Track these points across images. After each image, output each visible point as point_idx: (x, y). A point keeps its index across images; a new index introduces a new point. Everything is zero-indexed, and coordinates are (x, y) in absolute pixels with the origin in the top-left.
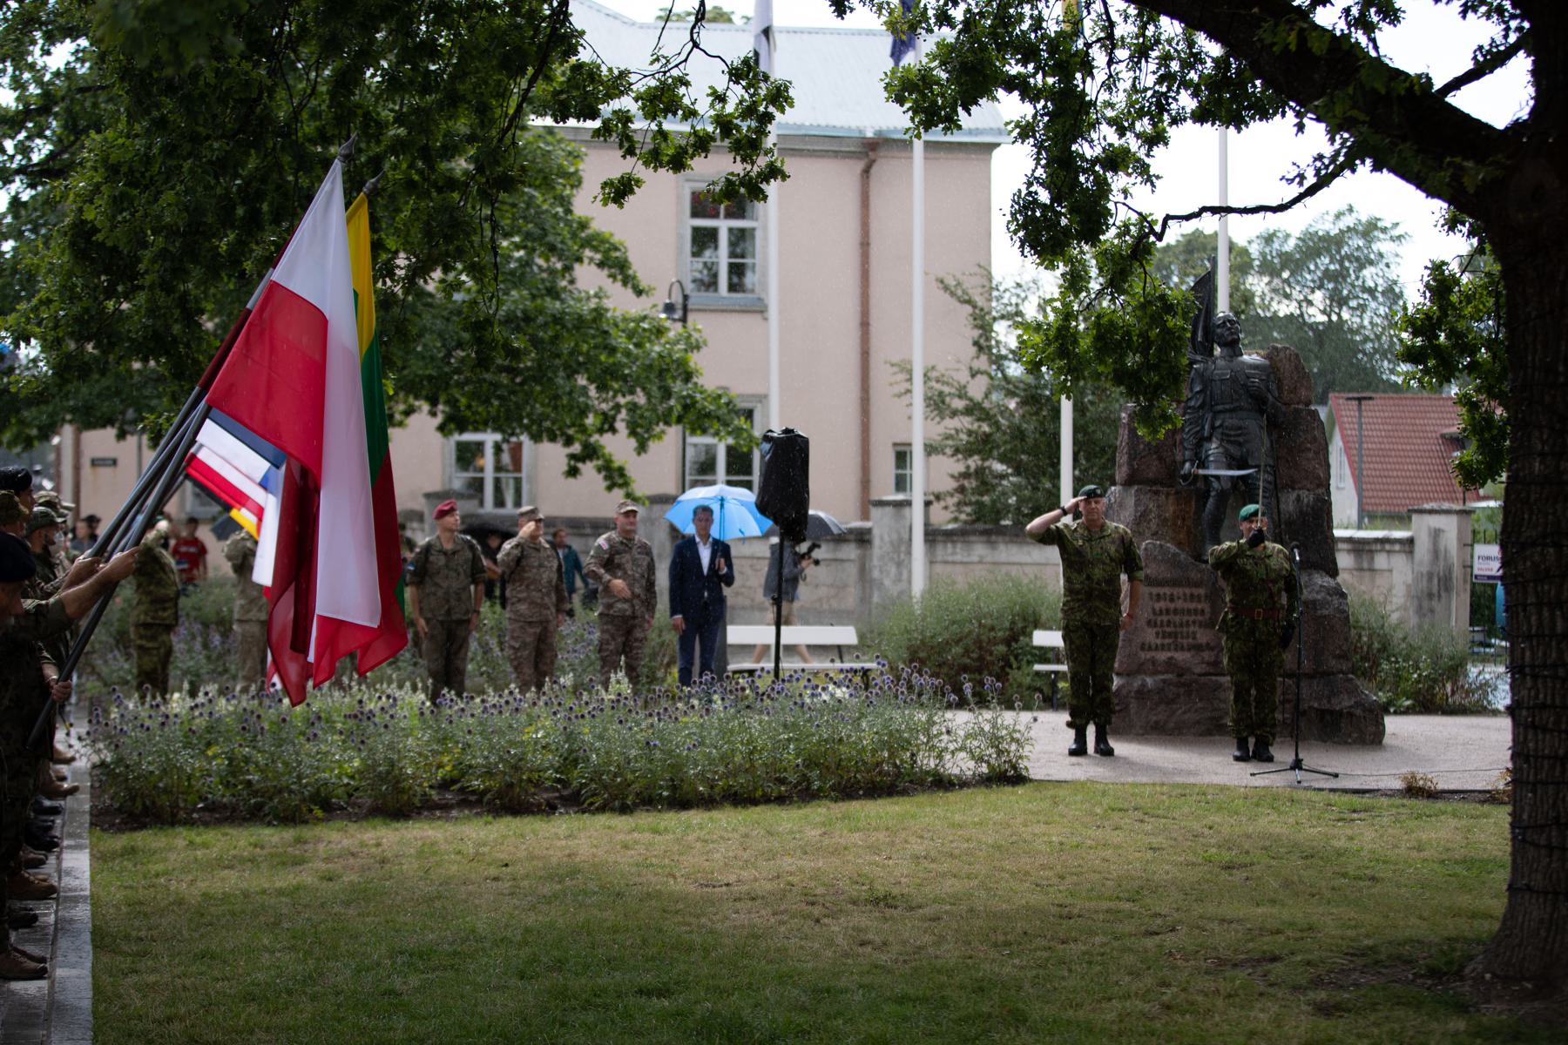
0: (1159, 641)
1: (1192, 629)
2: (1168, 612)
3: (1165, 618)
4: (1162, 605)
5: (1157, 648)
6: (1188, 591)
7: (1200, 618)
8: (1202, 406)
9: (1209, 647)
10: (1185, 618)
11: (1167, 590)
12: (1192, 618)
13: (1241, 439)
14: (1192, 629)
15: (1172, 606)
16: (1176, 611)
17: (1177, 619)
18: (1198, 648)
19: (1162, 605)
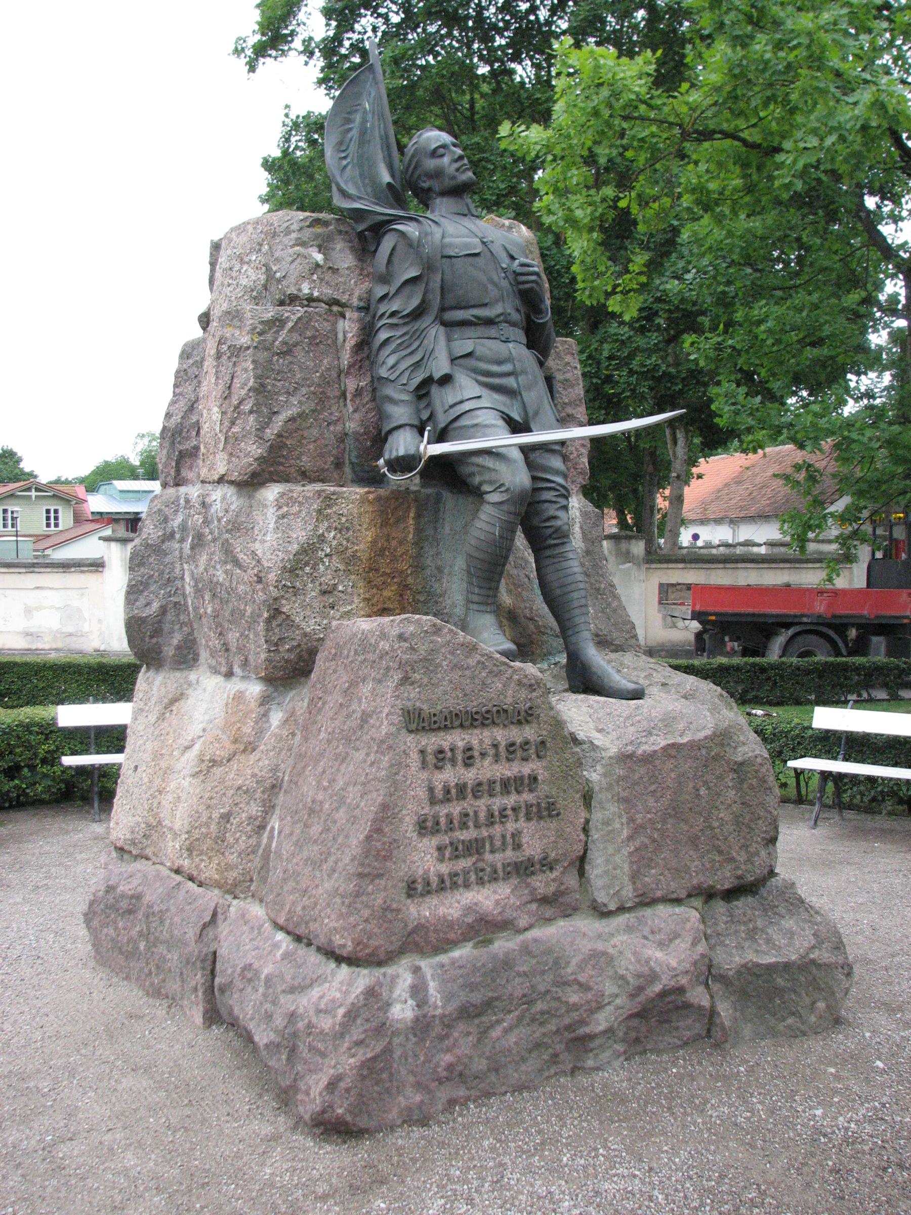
0: (445, 868)
1: (511, 826)
2: (461, 789)
3: (456, 809)
4: (449, 776)
5: (442, 887)
6: (501, 735)
7: (527, 797)
8: (417, 314)
9: (547, 864)
10: (497, 803)
11: (457, 739)
12: (511, 800)
13: (511, 382)
14: (511, 826)
15: (470, 776)
16: (478, 790)
17: (482, 804)
18: (523, 869)
19: (449, 776)
